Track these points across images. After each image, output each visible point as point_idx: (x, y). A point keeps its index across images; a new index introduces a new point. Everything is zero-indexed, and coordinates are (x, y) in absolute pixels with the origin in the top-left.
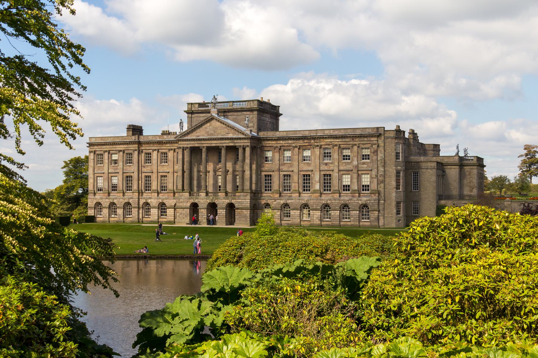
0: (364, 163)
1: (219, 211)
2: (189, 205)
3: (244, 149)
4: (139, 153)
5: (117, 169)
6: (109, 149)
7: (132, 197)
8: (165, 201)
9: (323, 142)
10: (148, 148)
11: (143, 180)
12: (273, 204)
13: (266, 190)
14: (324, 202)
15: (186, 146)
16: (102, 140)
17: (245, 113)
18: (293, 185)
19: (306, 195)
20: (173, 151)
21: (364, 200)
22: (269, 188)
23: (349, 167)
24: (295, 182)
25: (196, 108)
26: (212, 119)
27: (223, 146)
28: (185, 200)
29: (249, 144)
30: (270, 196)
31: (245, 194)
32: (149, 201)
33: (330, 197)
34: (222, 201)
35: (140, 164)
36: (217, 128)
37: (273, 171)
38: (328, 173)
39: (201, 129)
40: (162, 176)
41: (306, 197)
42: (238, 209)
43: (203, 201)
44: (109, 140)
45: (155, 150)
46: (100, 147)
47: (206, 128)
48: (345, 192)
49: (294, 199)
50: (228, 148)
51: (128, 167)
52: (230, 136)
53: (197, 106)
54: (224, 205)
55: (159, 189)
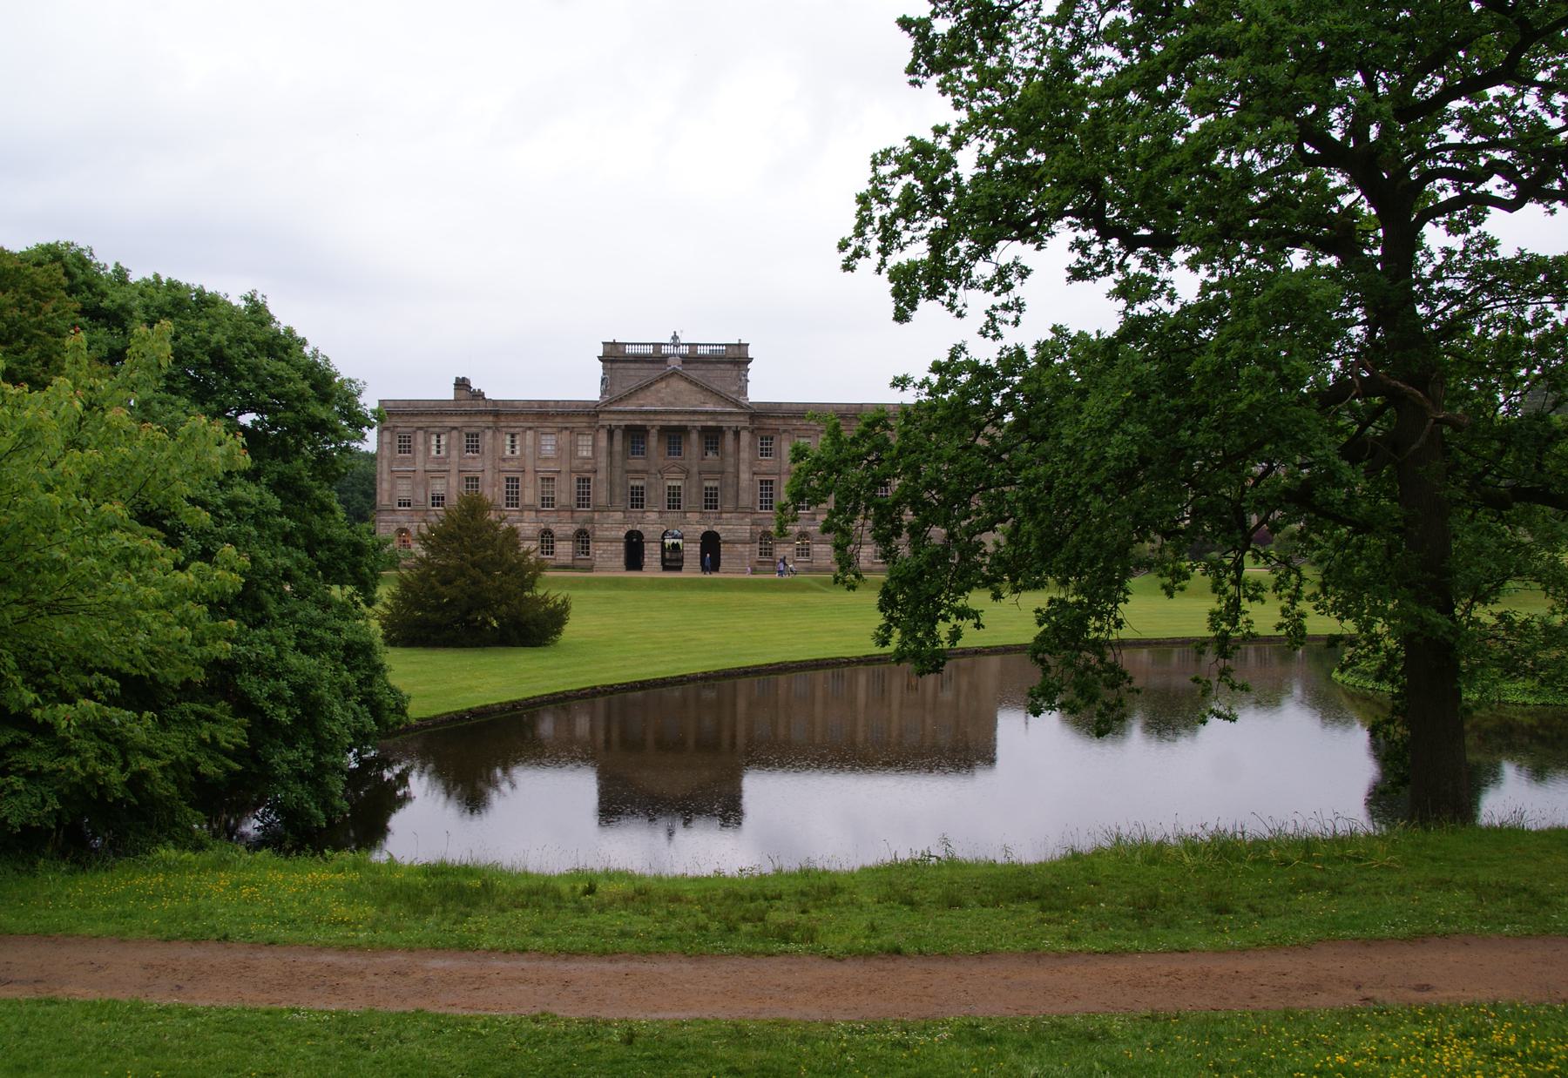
2: (622, 534)
3: (737, 433)
8: (552, 527)
15: (614, 423)
26: (674, 373)
28: (612, 528)
34: (695, 526)
46: (406, 418)
50: (705, 431)
52: (709, 407)
54: (698, 535)
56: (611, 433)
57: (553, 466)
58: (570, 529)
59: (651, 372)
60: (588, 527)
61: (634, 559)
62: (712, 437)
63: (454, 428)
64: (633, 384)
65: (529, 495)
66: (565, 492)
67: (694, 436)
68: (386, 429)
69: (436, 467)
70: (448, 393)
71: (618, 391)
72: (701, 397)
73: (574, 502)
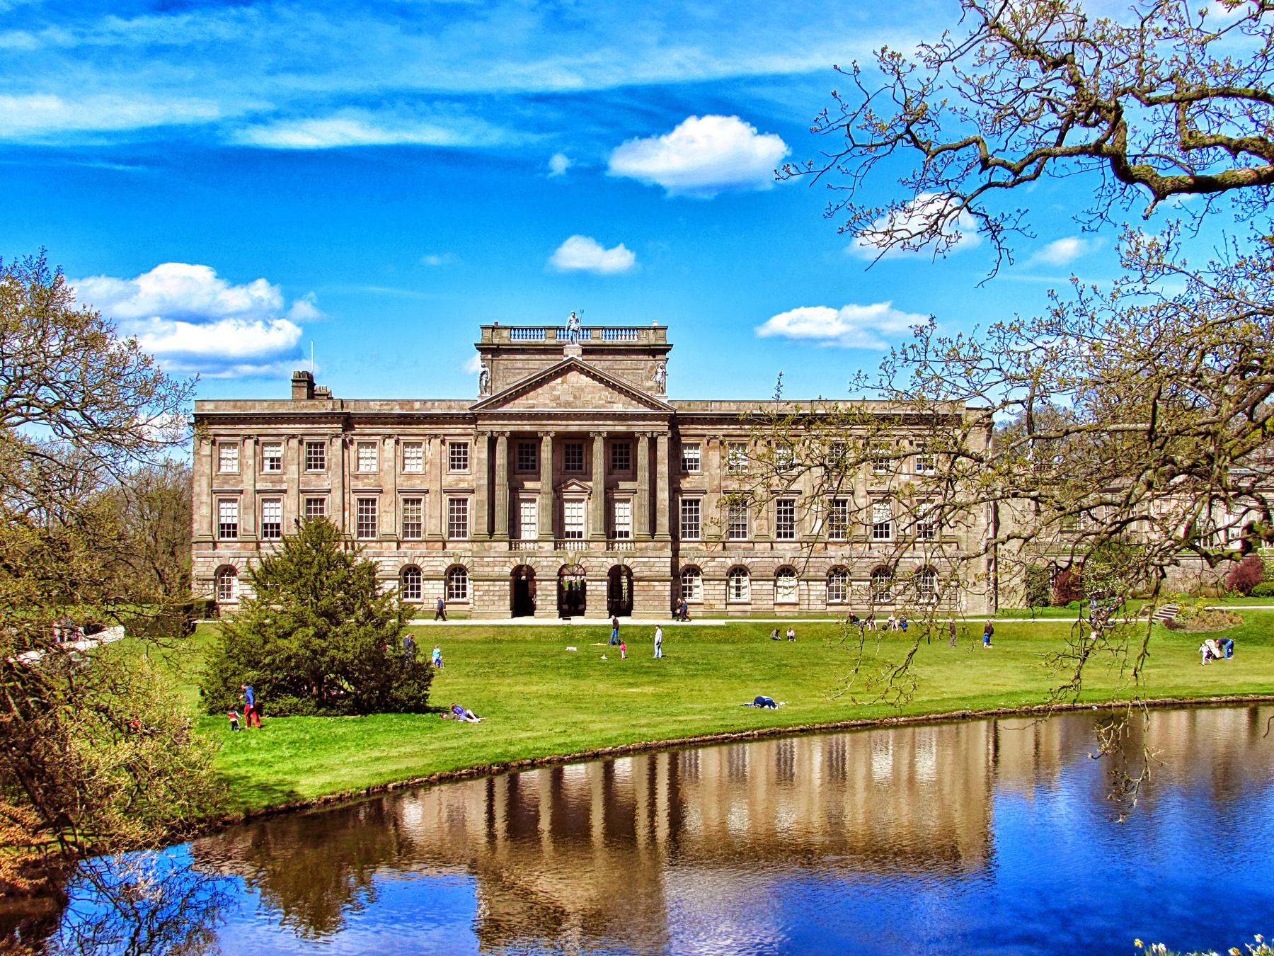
2: (508, 570)
3: (653, 443)
4: (345, 445)
5: (282, 482)
6: (258, 432)
8: (418, 562)
10: (367, 431)
11: (355, 510)
12: (708, 567)
13: (684, 536)
14: (833, 562)
15: (498, 429)
16: (235, 407)
18: (755, 524)
19: (786, 546)
20: (438, 441)
22: (694, 530)
25: (504, 338)
27: (600, 433)
28: (498, 561)
29: (666, 429)
30: (697, 549)
31: (659, 545)
33: (846, 550)
34: (600, 562)
35: (346, 469)
36: (581, 389)
37: (705, 493)
39: (540, 390)
40: (406, 501)
41: (787, 552)
42: (639, 580)
43: (546, 562)
44: (258, 409)
45: (390, 436)
47: (554, 388)
48: (879, 539)
49: (761, 558)
50: (611, 438)
51: (313, 477)
55: (399, 531)
56: (492, 443)
57: (418, 484)
58: (441, 564)
60: (464, 562)
61: (523, 603)
62: (622, 450)
63: (294, 436)
64: (521, 378)
65: (388, 519)
66: (434, 517)
67: (598, 446)
68: (204, 437)
69: (269, 486)
71: (500, 388)
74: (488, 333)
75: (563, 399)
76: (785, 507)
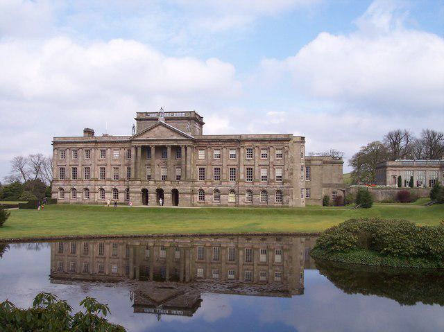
0: (278, 160)
1: (165, 195)
2: (140, 190)
3: (186, 148)
7: (92, 185)
9: (247, 144)
15: (137, 145)
17: (184, 121)
21: (278, 186)
23: (267, 163)
24: (226, 173)
28: (137, 188)
32: (104, 187)
38: (250, 167)
43: (152, 188)
50: (173, 148)
53: (144, 115)
54: (170, 191)
56: (136, 148)
57: (118, 163)
59: (153, 124)
66: (123, 173)
70: (81, 134)
72: (171, 133)
73: (125, 177)
74: (139, 114)
75: (158, 134)
76: (234, 171)
